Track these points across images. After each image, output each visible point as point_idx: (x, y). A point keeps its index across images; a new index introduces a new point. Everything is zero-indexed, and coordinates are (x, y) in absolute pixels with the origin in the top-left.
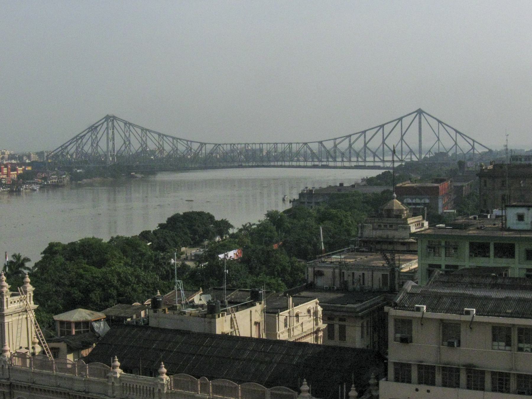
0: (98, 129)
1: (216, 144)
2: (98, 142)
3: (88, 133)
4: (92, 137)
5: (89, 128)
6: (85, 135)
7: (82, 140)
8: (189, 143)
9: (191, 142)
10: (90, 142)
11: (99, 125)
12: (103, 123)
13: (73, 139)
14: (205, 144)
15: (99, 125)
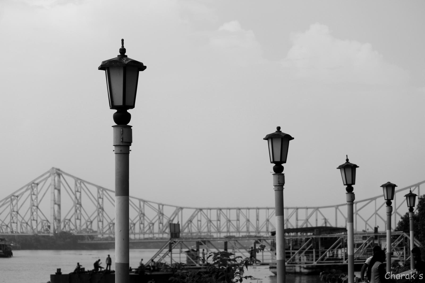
0: (40, 186)
1: (197, 209)
2: (38, 204)
3: (27, 190)
4: (31, 197)
5: (28, 185)
6: (22, 194)
7: (18, 201)
8: (161, 206)
9: (163, 205)
10: (28, 203)
11: (41, 182)
12: (46, 179)
13: (7, 199)
14: (182, 208)
15: (41, 182)
